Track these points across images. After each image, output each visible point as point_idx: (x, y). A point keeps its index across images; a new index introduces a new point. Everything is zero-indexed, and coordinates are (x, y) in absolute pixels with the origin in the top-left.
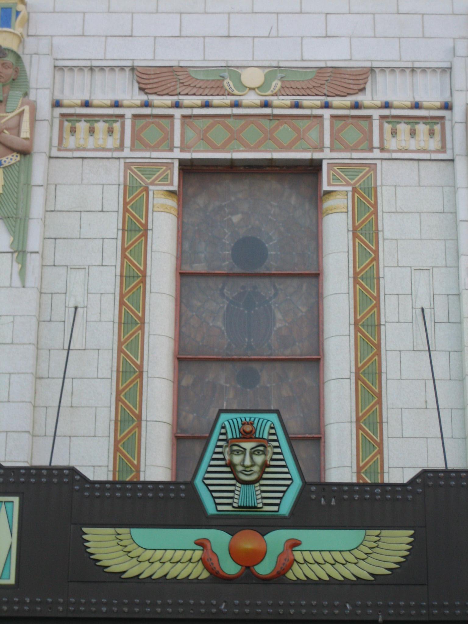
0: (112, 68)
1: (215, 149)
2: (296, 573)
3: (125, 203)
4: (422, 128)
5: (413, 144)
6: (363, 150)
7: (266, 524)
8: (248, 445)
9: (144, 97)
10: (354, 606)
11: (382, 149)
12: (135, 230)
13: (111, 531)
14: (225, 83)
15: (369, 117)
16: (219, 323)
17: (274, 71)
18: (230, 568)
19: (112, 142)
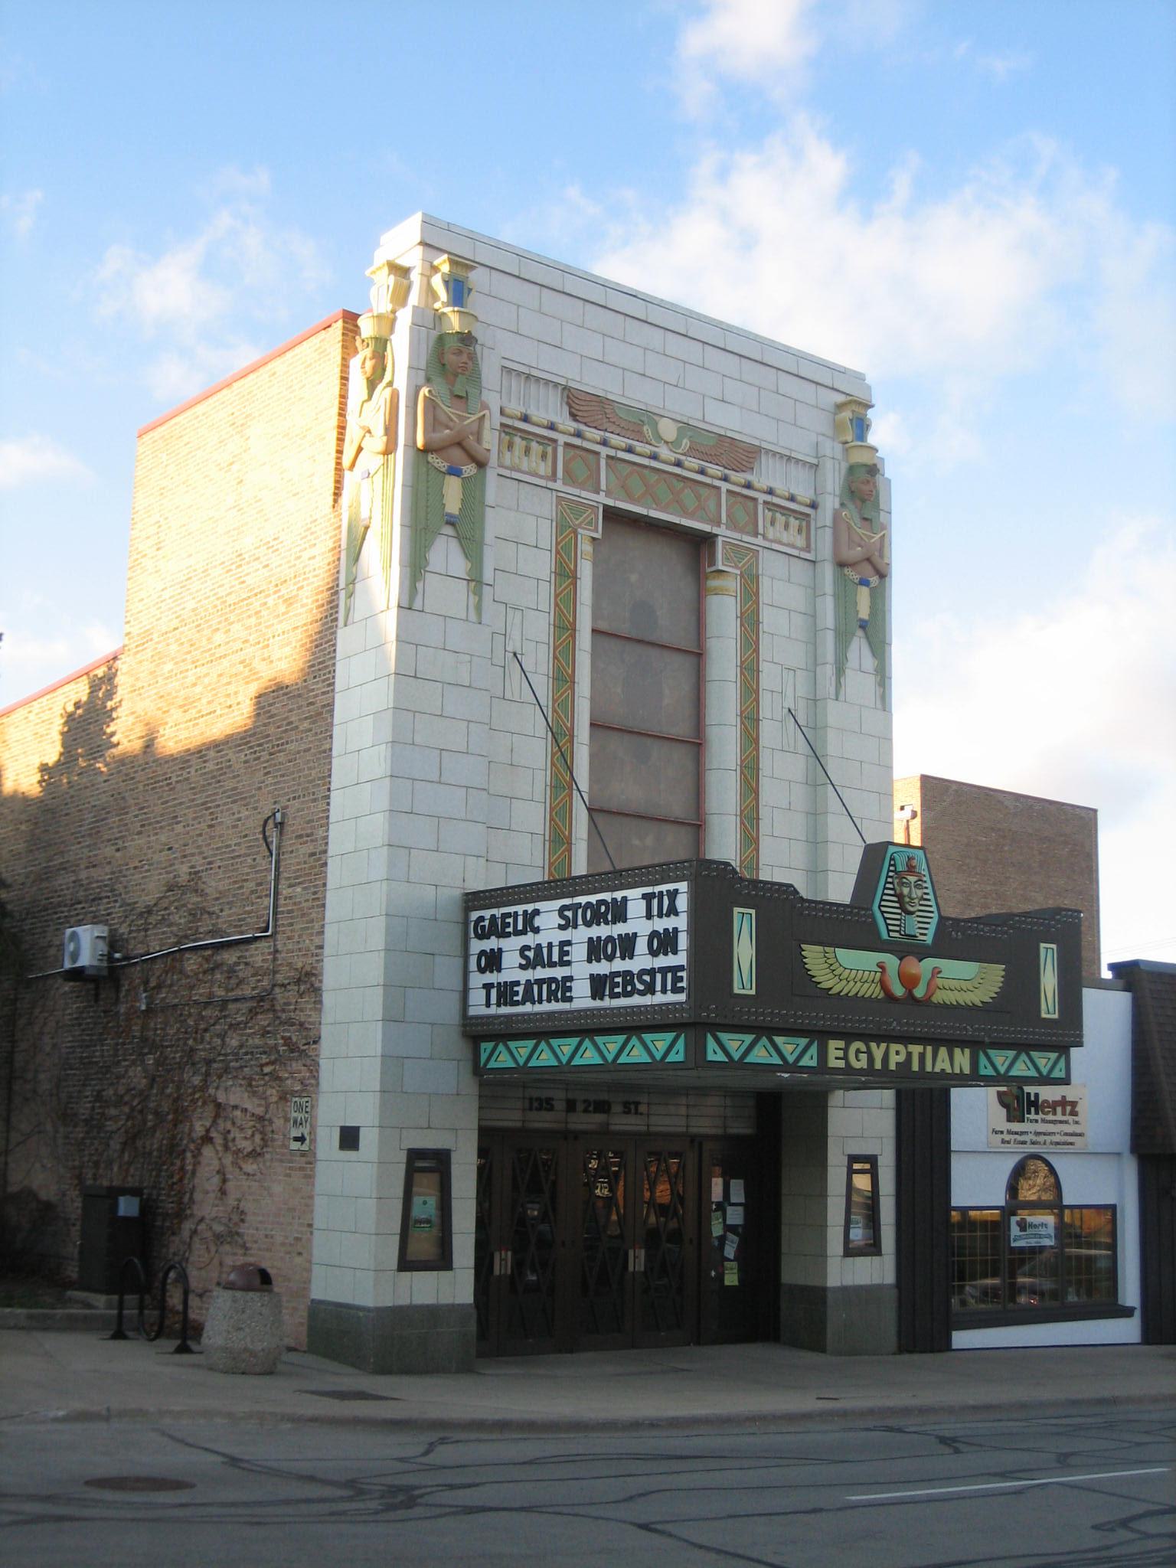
0: (547, 382)
1: (631, 499)
2: (939, 997)
3: (557, 544)
4: (794, 523)
5: (785, 537)
6: (748, 533)
7: (922, 952)
8: (913, 879)
9: (575, 425)
10: (975, 1030)
11: (764, 536)
12: (565, 574)
13: (820, 948)
14: (645, 428)
15: (755, 500)
16: (619, 690)
17: (685, 427)
18: (899, 991)
19: (544, 468)
